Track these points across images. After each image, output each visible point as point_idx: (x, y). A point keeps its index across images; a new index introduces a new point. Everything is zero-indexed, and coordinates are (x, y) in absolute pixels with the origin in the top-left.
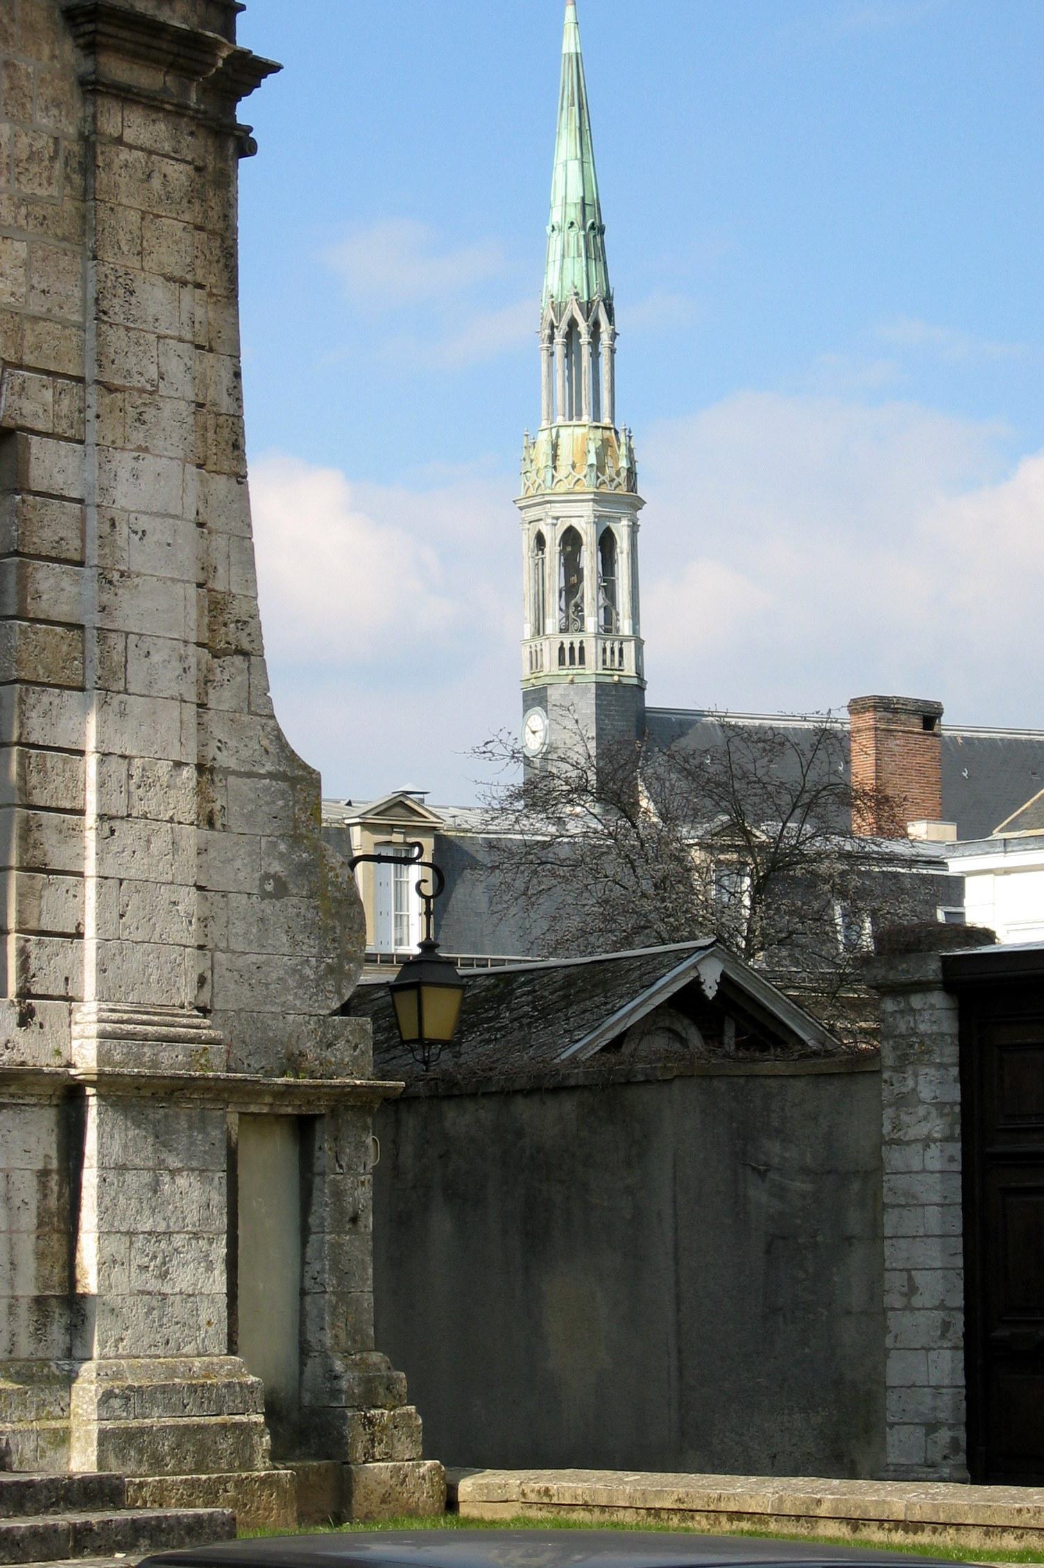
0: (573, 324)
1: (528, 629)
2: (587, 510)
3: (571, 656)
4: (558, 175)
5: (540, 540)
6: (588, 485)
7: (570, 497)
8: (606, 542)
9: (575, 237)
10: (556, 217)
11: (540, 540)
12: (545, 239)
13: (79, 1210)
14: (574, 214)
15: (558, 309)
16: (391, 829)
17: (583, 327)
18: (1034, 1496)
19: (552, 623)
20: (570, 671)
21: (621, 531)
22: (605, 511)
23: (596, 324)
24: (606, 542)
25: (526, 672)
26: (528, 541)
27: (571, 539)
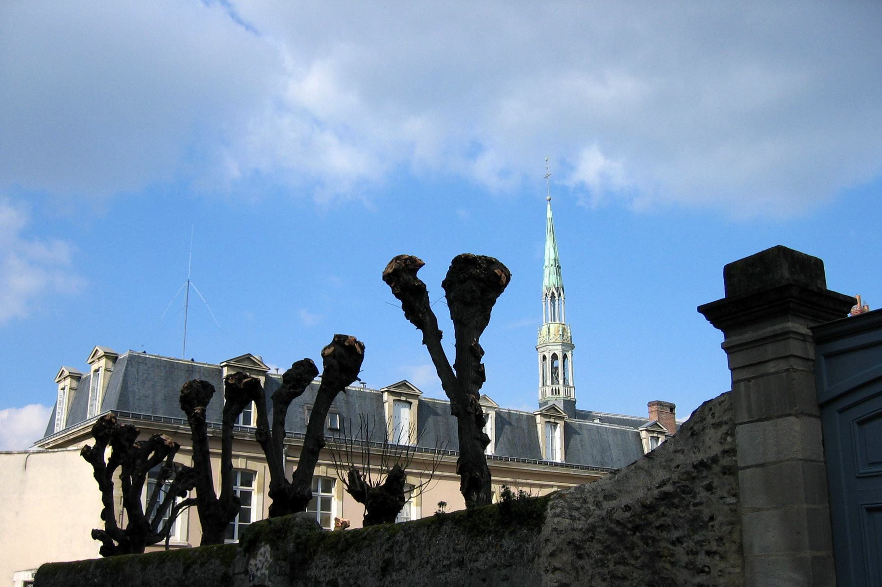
0: (553, 293)
1: (541, 384)
2: (560, 347)
3: (555, 392)
4: (547, 252)
5: (544, 358)
6: (560, 340)
7: (554, 344)
8: (565, 357)
9: (553, 269)
10: (547, 263)
11: (544, 358)
12: (543, 270)
13: (123, 486)
14: (552, 262)
15: (549, 289)
16: (550, 416)
17: (556, 295)
18: (125, 528)
19: (549, 382)
20: (555, 396)
21: (569, 354)
22: (565, 348)
23: (560, 295)
24: (565, 357)
25: (540, 397)
26: (540, 358)
27: (554, 357)
